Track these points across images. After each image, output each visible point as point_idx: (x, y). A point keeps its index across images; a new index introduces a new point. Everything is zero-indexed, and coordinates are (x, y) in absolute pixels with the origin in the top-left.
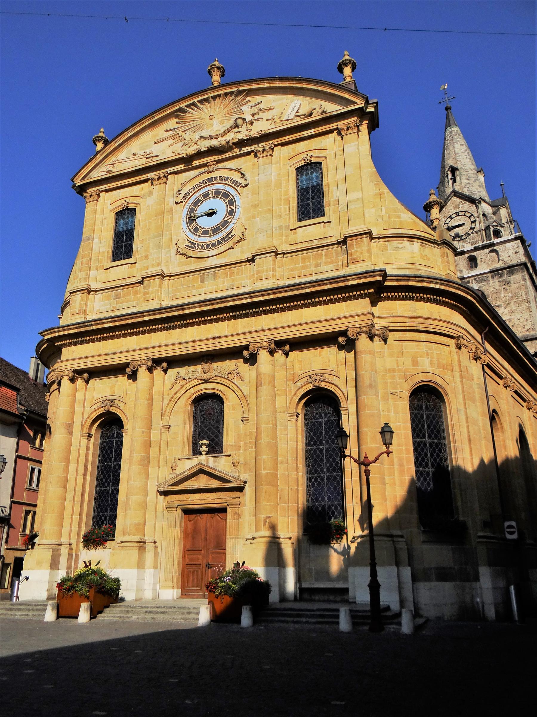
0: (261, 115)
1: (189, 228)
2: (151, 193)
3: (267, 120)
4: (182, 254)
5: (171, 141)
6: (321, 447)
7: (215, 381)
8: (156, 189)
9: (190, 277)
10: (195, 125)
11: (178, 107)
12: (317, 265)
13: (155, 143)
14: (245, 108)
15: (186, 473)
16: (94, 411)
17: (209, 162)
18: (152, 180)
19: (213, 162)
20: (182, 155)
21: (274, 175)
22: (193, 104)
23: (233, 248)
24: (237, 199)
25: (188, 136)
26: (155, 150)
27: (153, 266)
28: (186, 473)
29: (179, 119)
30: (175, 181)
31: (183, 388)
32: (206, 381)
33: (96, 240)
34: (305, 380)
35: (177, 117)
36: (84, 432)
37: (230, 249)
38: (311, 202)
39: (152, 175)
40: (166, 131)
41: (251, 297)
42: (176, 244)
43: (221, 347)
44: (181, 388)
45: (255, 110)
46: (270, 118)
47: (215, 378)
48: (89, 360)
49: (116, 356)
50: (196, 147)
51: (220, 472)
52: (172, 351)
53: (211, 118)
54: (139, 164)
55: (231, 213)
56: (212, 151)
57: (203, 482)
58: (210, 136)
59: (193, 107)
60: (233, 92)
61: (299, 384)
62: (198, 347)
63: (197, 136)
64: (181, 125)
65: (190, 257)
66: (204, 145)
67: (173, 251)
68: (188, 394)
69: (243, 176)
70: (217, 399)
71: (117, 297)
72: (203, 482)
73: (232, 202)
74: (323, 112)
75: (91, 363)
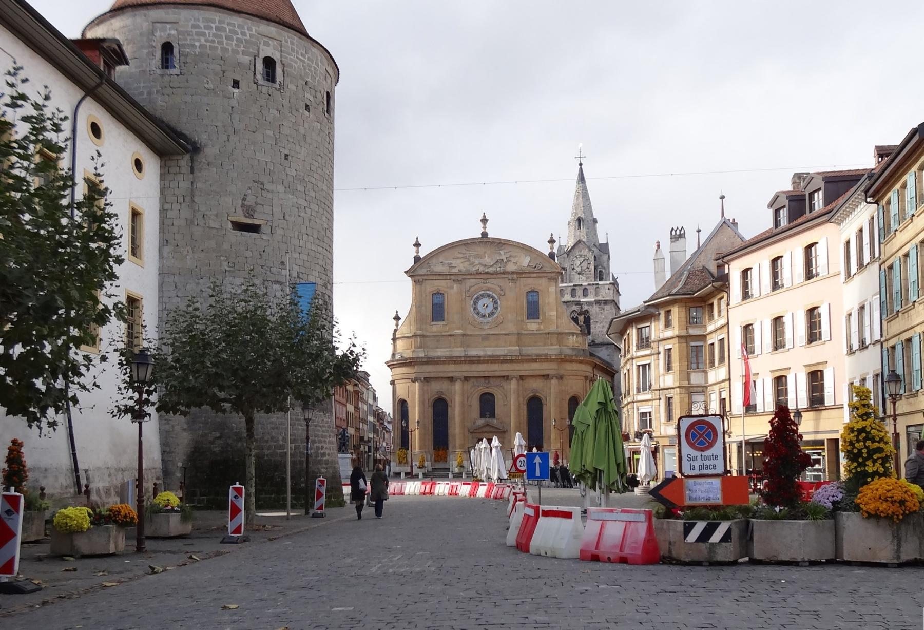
2: (452, 288)
8: (455, 286)
14: (502, 252)
25: (472, 259)
38: (533, 311)
39: (452, 277)
50: (477, 268)
55: (496, 308)
57: (487, 429)
63: (477, 262)
66: (481, 269)
70: (492, 395)
71: (438, 341)
73: (496, 303)
75: (432, 375)
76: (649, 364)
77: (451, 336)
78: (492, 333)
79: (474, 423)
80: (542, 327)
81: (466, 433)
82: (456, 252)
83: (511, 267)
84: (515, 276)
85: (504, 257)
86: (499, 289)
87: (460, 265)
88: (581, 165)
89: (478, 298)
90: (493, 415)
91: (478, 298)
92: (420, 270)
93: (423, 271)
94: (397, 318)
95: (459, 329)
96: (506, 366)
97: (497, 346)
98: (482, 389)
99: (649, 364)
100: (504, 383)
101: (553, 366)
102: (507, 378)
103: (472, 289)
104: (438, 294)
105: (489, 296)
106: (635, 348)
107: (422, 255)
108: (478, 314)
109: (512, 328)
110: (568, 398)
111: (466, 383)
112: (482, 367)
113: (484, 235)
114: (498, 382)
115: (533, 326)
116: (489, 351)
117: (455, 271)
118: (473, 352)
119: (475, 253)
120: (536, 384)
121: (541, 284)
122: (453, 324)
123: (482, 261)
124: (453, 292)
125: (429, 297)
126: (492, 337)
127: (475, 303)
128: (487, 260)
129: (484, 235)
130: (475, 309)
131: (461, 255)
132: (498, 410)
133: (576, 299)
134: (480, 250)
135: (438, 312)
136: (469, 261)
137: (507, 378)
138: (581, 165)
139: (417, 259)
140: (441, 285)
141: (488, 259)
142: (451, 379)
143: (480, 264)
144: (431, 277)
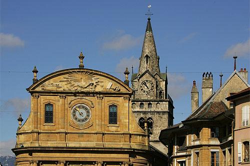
0: (99, 83)
2: (59, 101)
8: (61, 100)
9: (75, 135)
14: (93, 78)
21: (101, 107)
25: (73, 83)
26: (60, 84)
27: (61, 128)
45: (97, 81)
53: (82, 78)
54: (54, 89)
55: (88, 116)
56: (82, 93)
66: (79, 89)
71: (48, 136)
73: (88, 112)
74: (120, 90)
75: (44, 159)
76: (185, 162)
77: (59, 133)
78: (85, 132)
83: (99, 89)
84: (102, 95)
85: (94, 83)
86: (90, 103)
88: (149, 19)
93: (39, 89)
94: (21, 120)
95: (64, 128)
96: (93, 155)
97: (88, 141)
99: (185, 162)
104: (49, 105)
105: (83, 107)
106: (176, 151)
107: (39, 76)
108: (76, 119)
109: (97, 129)
113: (81, 67)
115: (113, 128)
116: (83, 144)
117: (61, 90)
118: (72, 144)
119: (74, 78)
122: (58, 124)
123: (79, 84)
124: (58, 103)
125: (43, 107)
126: (85, 135)
127: (74, 112)
128: (83, 83)
129: (81, 67)
130: (74, 115)
131: (66, 80)
133: (144, 110)
134: (78, 76)
135: (49, 117)
136: (70, 83)
138: (149, 19)
139: (35, 81)
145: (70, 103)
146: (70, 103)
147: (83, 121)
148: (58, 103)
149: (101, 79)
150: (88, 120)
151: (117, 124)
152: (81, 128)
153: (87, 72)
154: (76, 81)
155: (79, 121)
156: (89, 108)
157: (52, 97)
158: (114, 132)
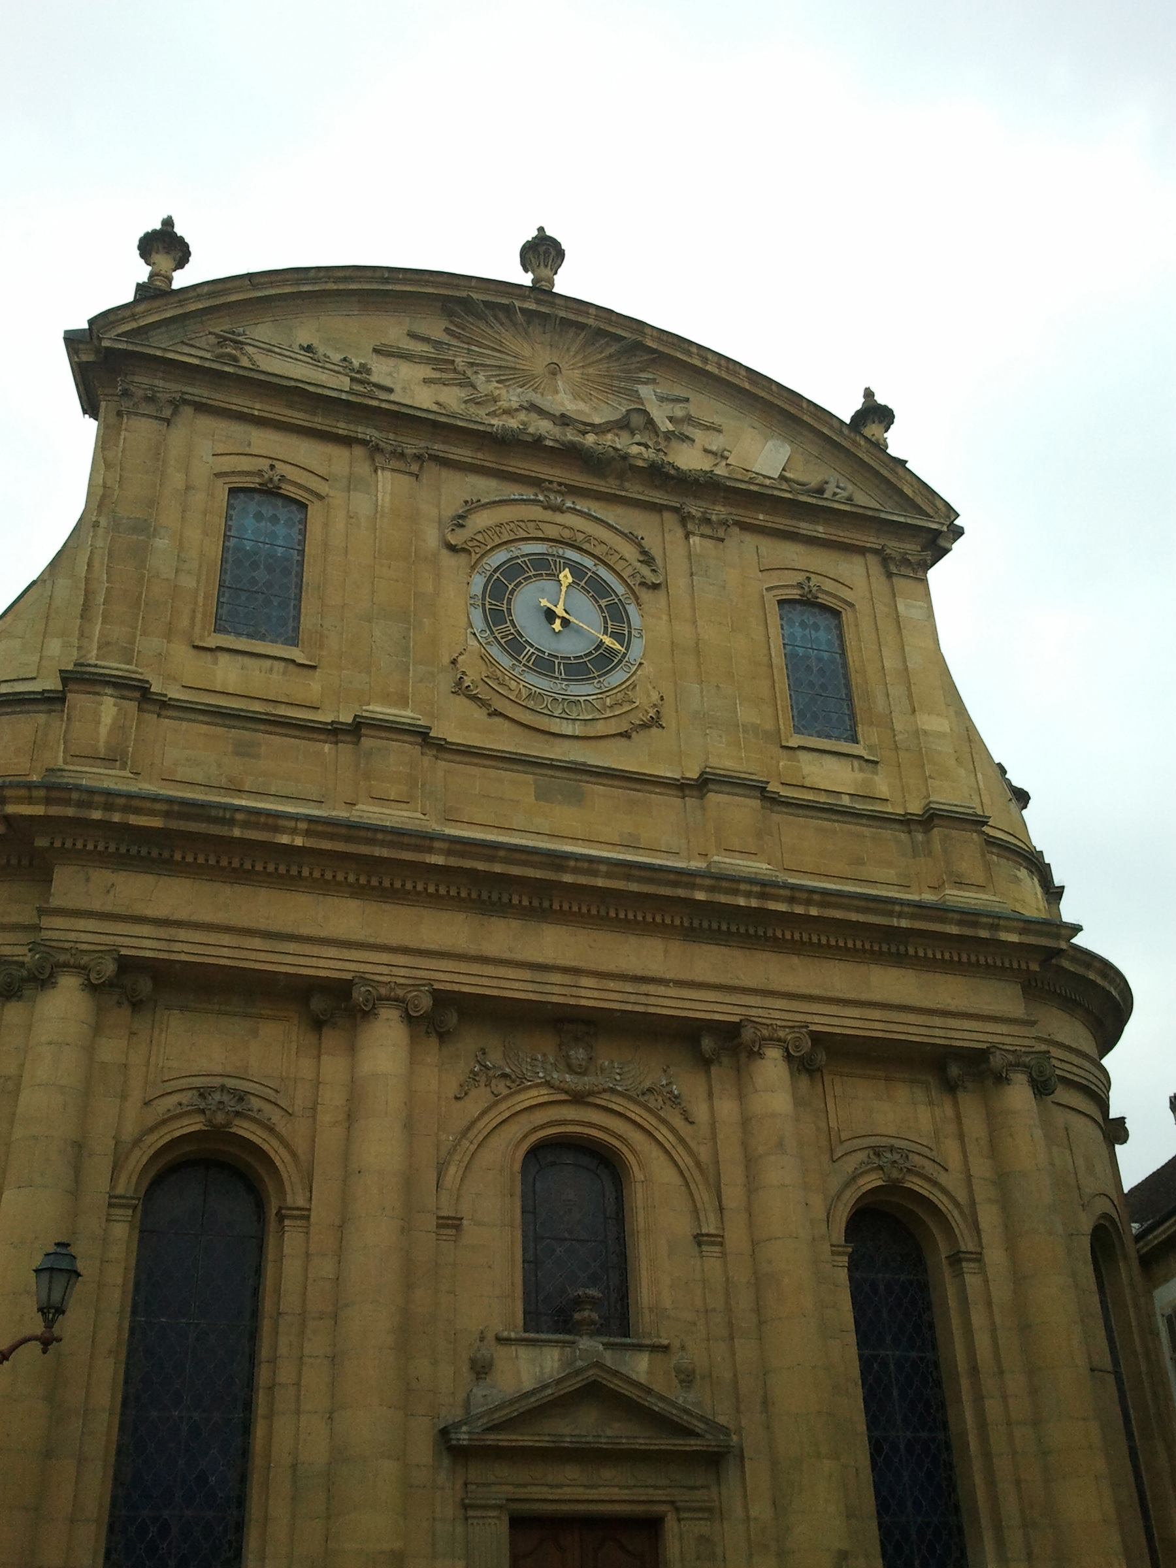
0: (689, 430)
1: (492, 633)
3: (706, 450)
4: (474, 698)
5: (427, 371)
6: (882, 1353)
7: (603, 1103)
8: (385, 480)
10: (503, 364)
11: (464, 294)
12: (860, 862)
13: (376, 351)
14: (645, 391)
15: (549, 1391)
16: (164, 1122)
17: (551, 482)
18: (377, 449)
19: (560, 484)
20: (489, 429)
22: (507, 309)
23: (629, 737)
24: (632, 609)
26: (381, 371)
28: (549, 1391)
29: (452, 322)
30: (458, 488)
31: (503, 1106)
32: (578, 1099)
33: (161, 543)
34: (861, 1156)
35: (449, 314)
36: (120, 1191)
37: (620, 735)
40: (412, 335)
41: (763, 896)
42: (454, 662)
43: (651, 1010)
44: (495, 1104)
46: (714, 448)
47: (606, 1096)
48: (182, 934)
49: (292, 947)
51: (662, 1398)
52: (495, 983)
53: (554, 370)
57: (586, 1426)
58: (563, 415)
59: (501, 316)
60: (620, 338)
61: (850, 1164)
62: (583, 993)
64: (454, 342)
65: (501, 715)
67: (445, 682)
68: (515, 1130)
69: (647, 559)
70: (603, 1162)
71: (243, 751)
72: (586, 1426)
74: (850, 499)
75: (189, 948)
79: (481, 1369)
80: (882, 785)
81: (423, 1449)
82: (394, 329)
84: (719, 511)
86: (629, 552)
87: (412, 387)
89: (514, 572)
90: (618, 1319)
91: (514, 572)
92: (153, 356)
98: (536, 1108)
100: (688, 1084)
101: (1000, 999)
102: (717, 1045)
103: (481, 520)
110: (1086, 1224)
111: (432, 1051)
112: (553, 944)
114: (648, 1069)
120: (898, 1114)
121: (852, 578)
123: (537, 399)
132: (663, 1276)
135: (260, 594)
137: (717, 1045)
140: (301, 458)
141: (571, 397)
142: (330, 1006)
143: (533, 408)
144: (238, 401)
145: (459, 522)
146: (459, 522)
147: (577, 670)
148: (363, 511)
149: (705, 406)
150: (617, 677)
151: (855, 740)
152: (567, 729)
153: (600, 333)
154: (508, 375)
155: (544, 664)
156: (620, 590)
157: (307, 452)
158: (846, 801)
